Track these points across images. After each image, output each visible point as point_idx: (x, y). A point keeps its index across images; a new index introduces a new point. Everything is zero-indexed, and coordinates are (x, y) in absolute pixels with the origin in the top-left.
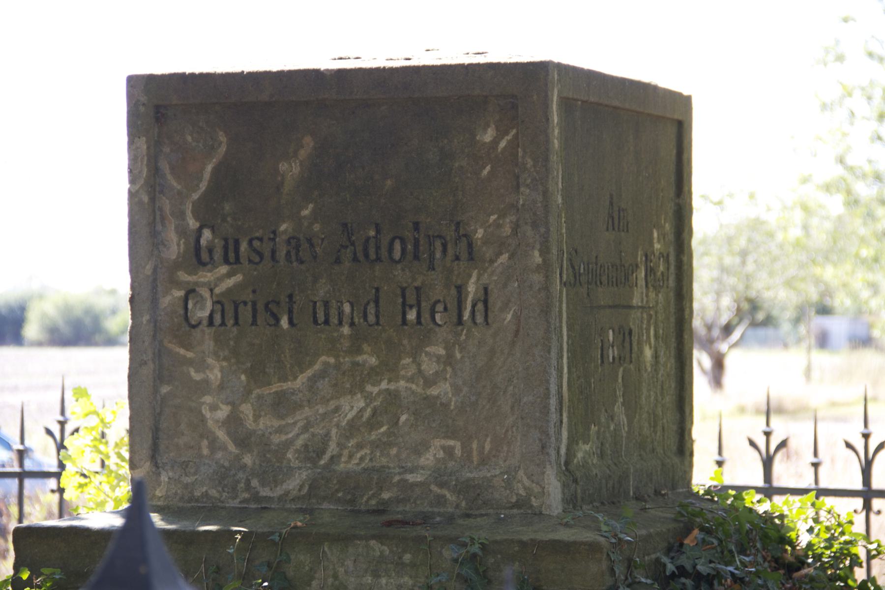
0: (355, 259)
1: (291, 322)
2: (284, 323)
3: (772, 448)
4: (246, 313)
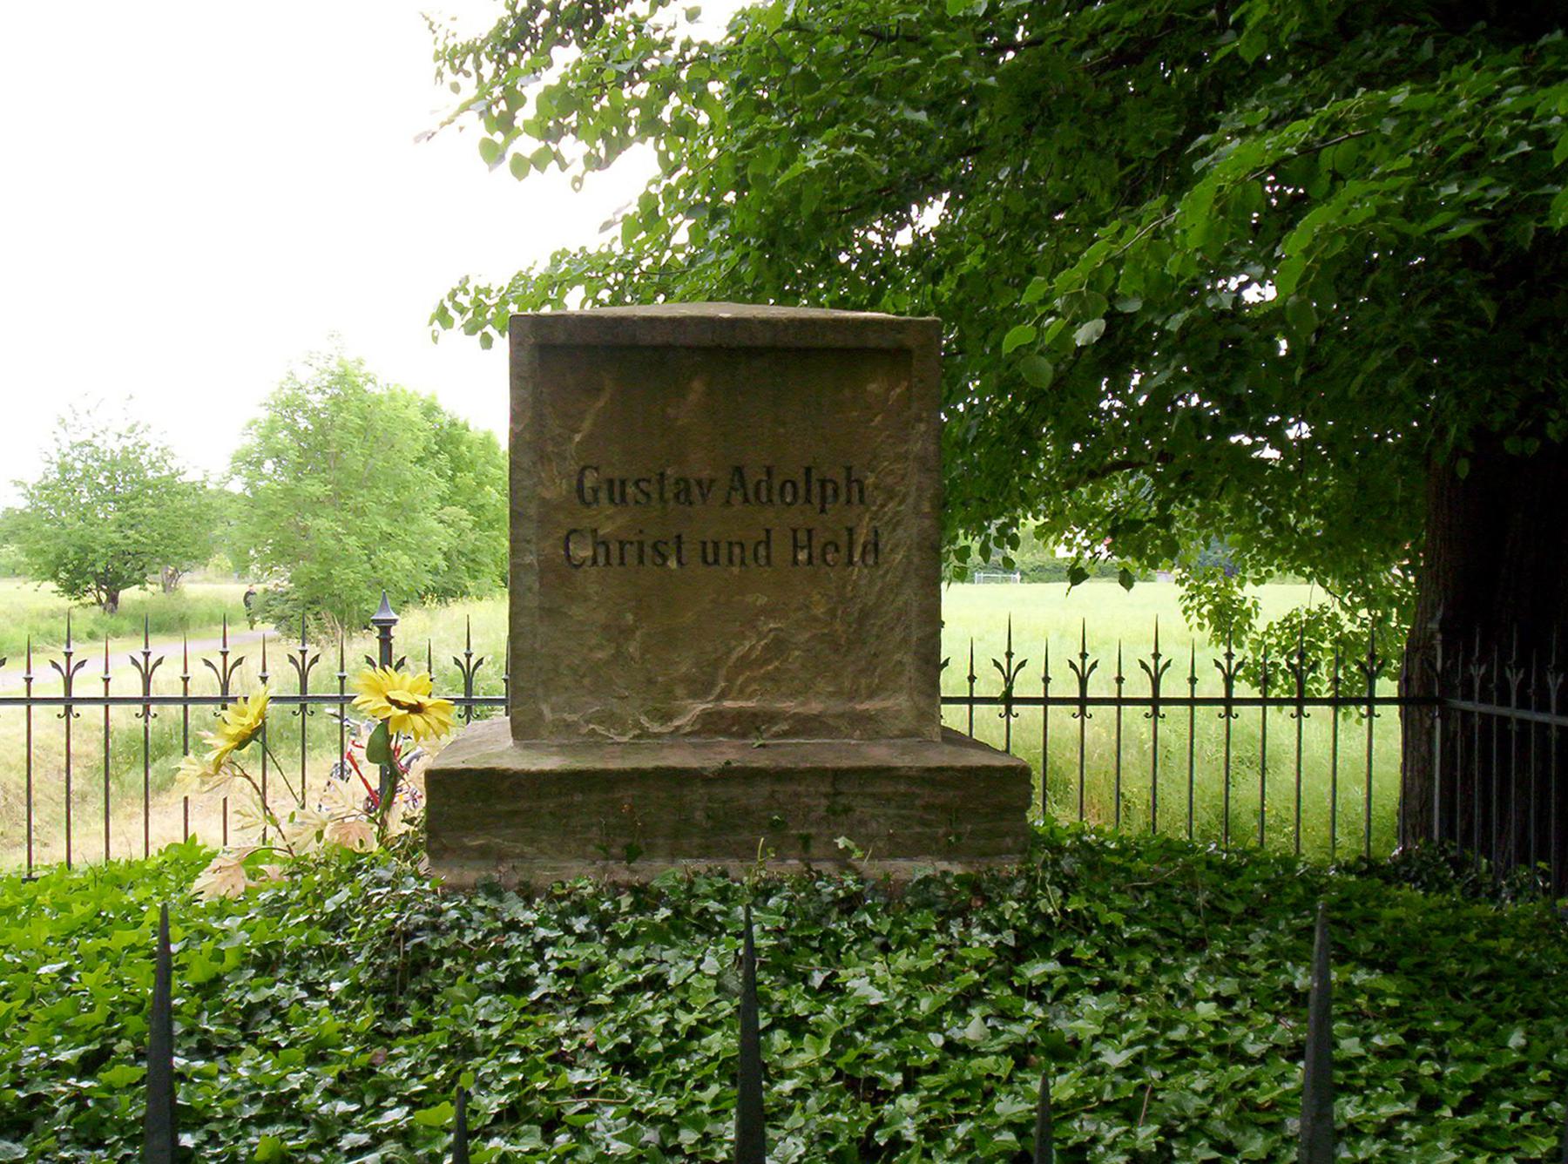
0: (746, 500)
1: (679, 561)
2: (672, 564)
3: (229, 667)
4: (631, 551)
